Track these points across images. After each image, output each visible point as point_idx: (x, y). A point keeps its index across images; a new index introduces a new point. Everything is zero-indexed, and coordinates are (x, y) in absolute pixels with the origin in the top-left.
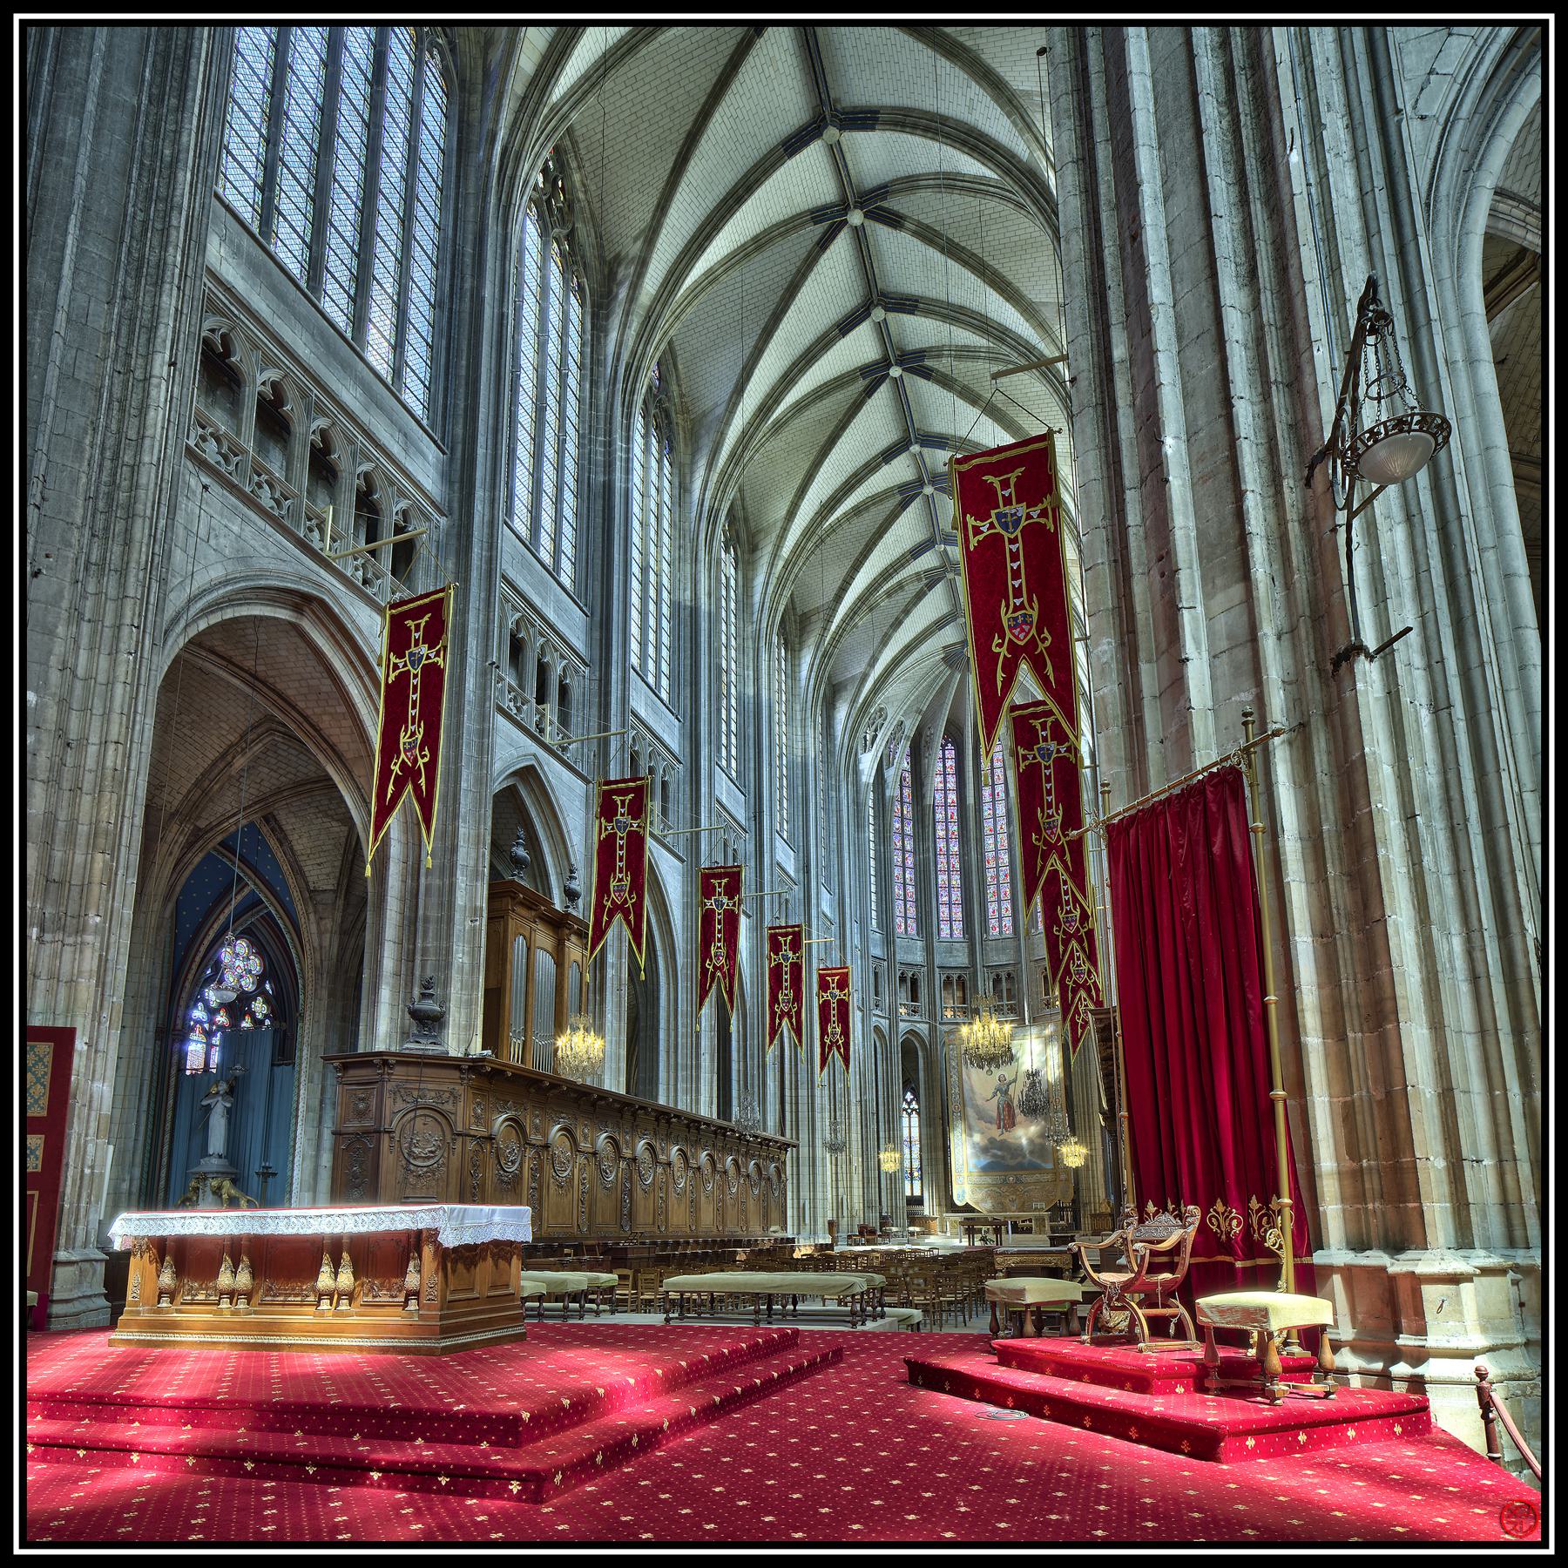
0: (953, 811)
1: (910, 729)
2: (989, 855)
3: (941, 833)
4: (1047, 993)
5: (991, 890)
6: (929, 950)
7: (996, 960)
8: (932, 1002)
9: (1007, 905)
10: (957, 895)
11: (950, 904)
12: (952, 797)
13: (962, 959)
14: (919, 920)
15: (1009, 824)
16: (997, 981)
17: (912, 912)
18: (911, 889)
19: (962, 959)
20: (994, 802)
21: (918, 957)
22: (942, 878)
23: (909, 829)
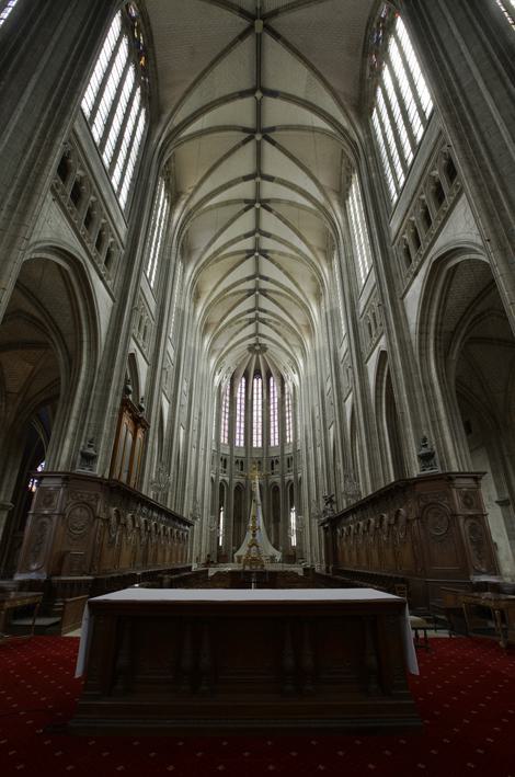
0: (243, 401)
2: (255, 419)
5: (255, 431)
6: (231, 449)
8: (231, 469)
9: (260, 437)
10: (242, 431)
12: (243, 396)
13: (243, 455)
14: (228, 438)
17: (226, 435)
18: (227, 427)
21: (227, 452)
22: (238, 424)
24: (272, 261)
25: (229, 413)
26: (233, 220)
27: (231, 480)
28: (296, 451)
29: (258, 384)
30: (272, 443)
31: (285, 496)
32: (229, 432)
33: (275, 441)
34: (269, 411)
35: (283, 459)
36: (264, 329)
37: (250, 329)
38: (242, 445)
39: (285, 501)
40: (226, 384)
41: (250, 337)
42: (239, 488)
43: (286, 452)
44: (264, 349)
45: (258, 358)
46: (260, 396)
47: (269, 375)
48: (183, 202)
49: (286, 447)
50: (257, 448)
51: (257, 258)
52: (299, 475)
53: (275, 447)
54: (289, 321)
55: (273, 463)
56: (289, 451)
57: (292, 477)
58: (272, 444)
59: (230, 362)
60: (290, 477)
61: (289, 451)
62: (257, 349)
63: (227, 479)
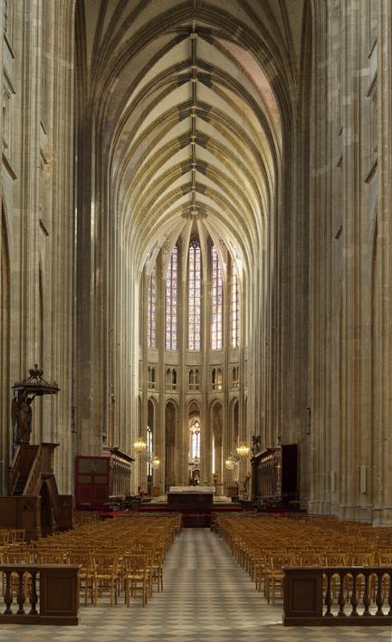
1: (160, 245)
2: (191, 308)
3: (168, 294)
4: (214, 382)
5: (191, 327)
6: (161, 356)
7: (193, 362)
9: (198, 336)
10: (174, 328)
11: (171, 332)
12: (175, 275)
13: (175, 361)
15: (202, 293)
16: (191, 372)
18: (154, 324)
19: (175, 361)
20: (195, 279)
22: (168, 318)
23: (154, 291)
24: (212, 152)
25: (156, 304)
26: (166, 131)
27: (161, 397)
28: (243, 361)
29: (194, 256)
30: (214, 343)
31: (229, 417)
32: (157, 331)
33: (216, 344)
34: (210, 298)
35: (227, 370)
36: (200, 197)
37: (186, 199)
38: (174, 347)
39: (229, 423)
40: (152, 264)
41: (184, 205)
42: (170, 406)
43: (232, 360)
44: (202, 210)
45: (195, 226)
46: (198, 274)
47: (210, 244)
48: (118, 153)
49: (231, 353)
50: (194, 352)
51: (193, 147)
52: (245, 392)
53: (216, 351)
54: (232, 202)
55: (214, 373)
56: (235, 359)
57: (237, 394)
58: (214, 348)
59: (159, 238)
60: (234, 393)
61: (235, 359)
62: (195, 211)
63: (157, 395)
